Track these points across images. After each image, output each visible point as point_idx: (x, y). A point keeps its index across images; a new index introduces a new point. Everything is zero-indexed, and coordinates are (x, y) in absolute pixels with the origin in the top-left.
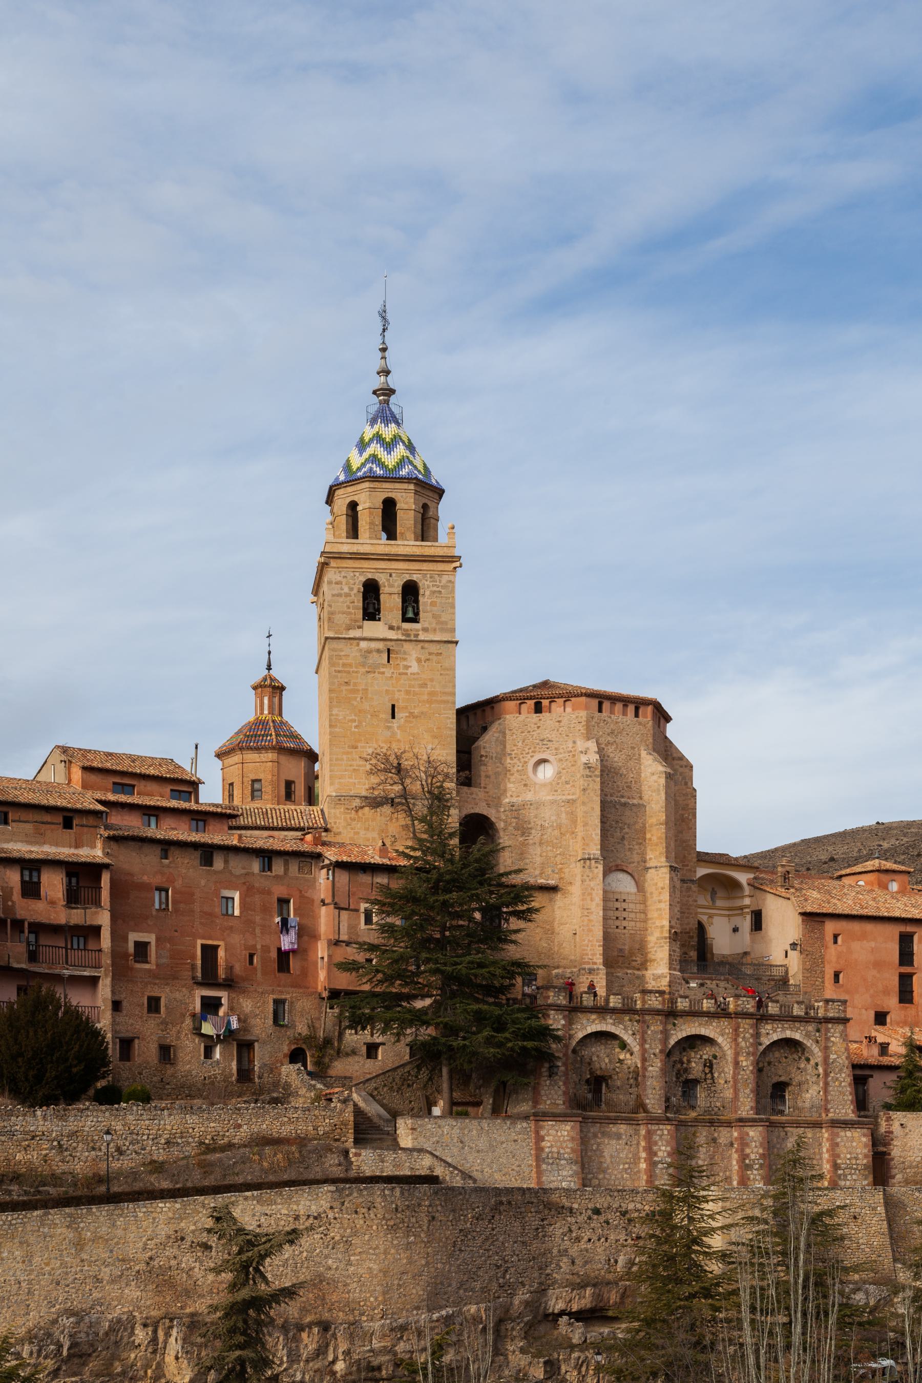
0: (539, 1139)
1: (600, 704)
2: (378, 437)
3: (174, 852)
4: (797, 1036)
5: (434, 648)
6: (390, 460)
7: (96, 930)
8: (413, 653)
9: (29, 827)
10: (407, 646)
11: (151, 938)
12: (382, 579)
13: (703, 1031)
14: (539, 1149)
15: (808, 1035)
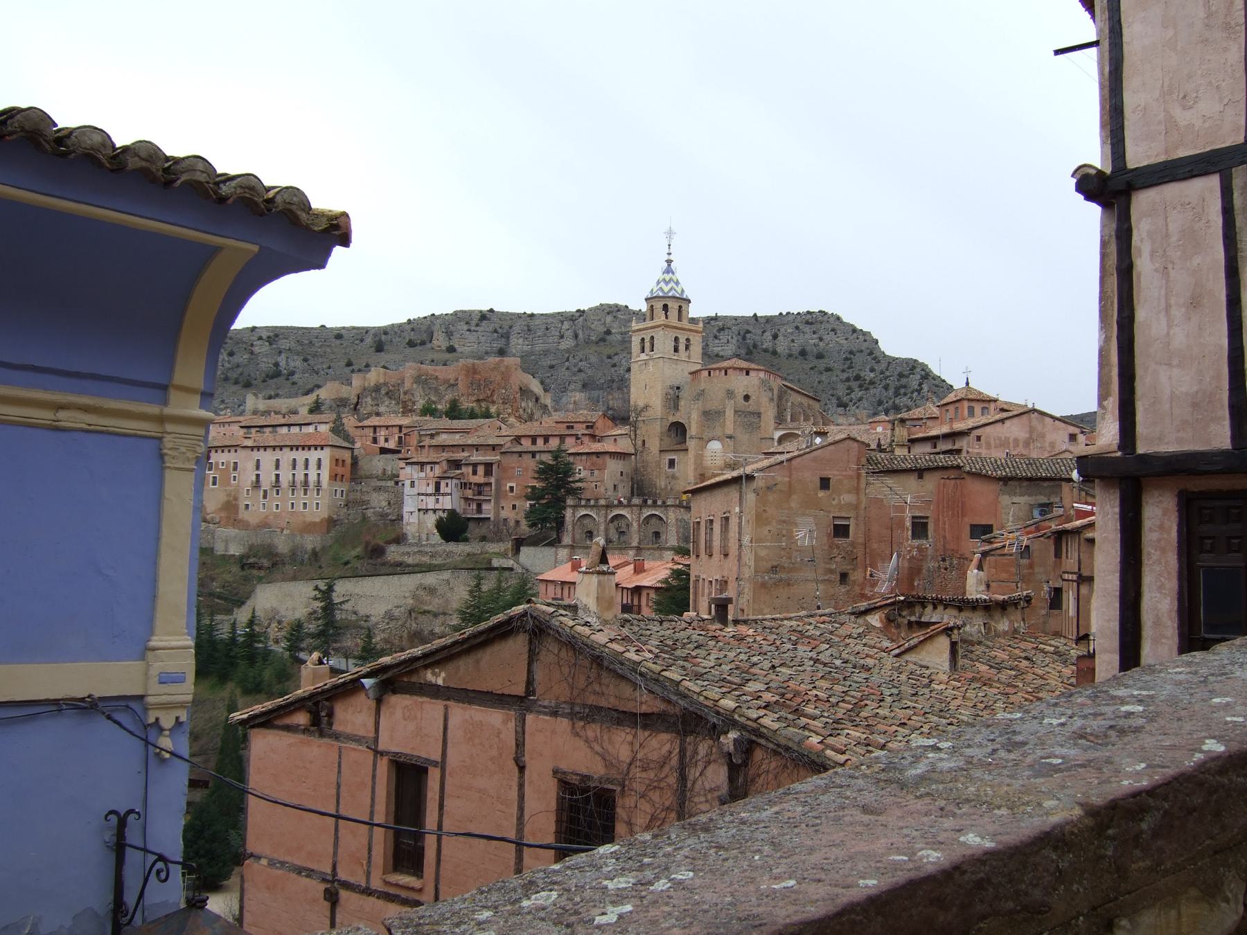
0: (557, 554)
1: (710, 373)
2: (664, 280)
3: (523, 455)
4: (657, 513)
5: (656, 360)
6: (666, 289)
7: (491, 484)
8: (651, 363)
9: (482, 452)
10: (650, 362)
11: (514, 485)
12: (644, 336)
13: (621, 513)
14: (556, 559)
15: (662, 512)
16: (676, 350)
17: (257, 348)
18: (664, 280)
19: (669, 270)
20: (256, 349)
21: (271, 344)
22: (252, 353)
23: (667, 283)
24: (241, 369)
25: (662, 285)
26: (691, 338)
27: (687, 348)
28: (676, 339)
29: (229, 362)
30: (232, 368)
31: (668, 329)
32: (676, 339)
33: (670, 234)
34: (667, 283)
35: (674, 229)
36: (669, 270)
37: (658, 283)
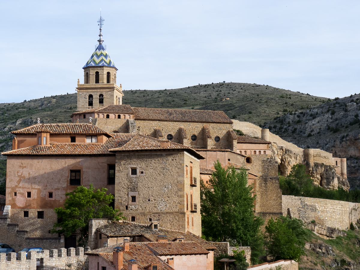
16: (91, 104)
17: (349, 107)
18: (97, 55)
19: (100, 47)
20: (349, 108)
21: (357, 104)
22: (346, 111)
23: (98, 57)
24: (338, 121)
25: (95, 58)
26: (104, 94)
27: (101, 101)
28: (91, 96)
29: (331, 118)
30: (333, 122)
31: (82, 91)
32: (91, 96)
33: (101, 21)
34: (98, 57)
35: (103, 18)
36: (100, 47)
37: (92, 56)
